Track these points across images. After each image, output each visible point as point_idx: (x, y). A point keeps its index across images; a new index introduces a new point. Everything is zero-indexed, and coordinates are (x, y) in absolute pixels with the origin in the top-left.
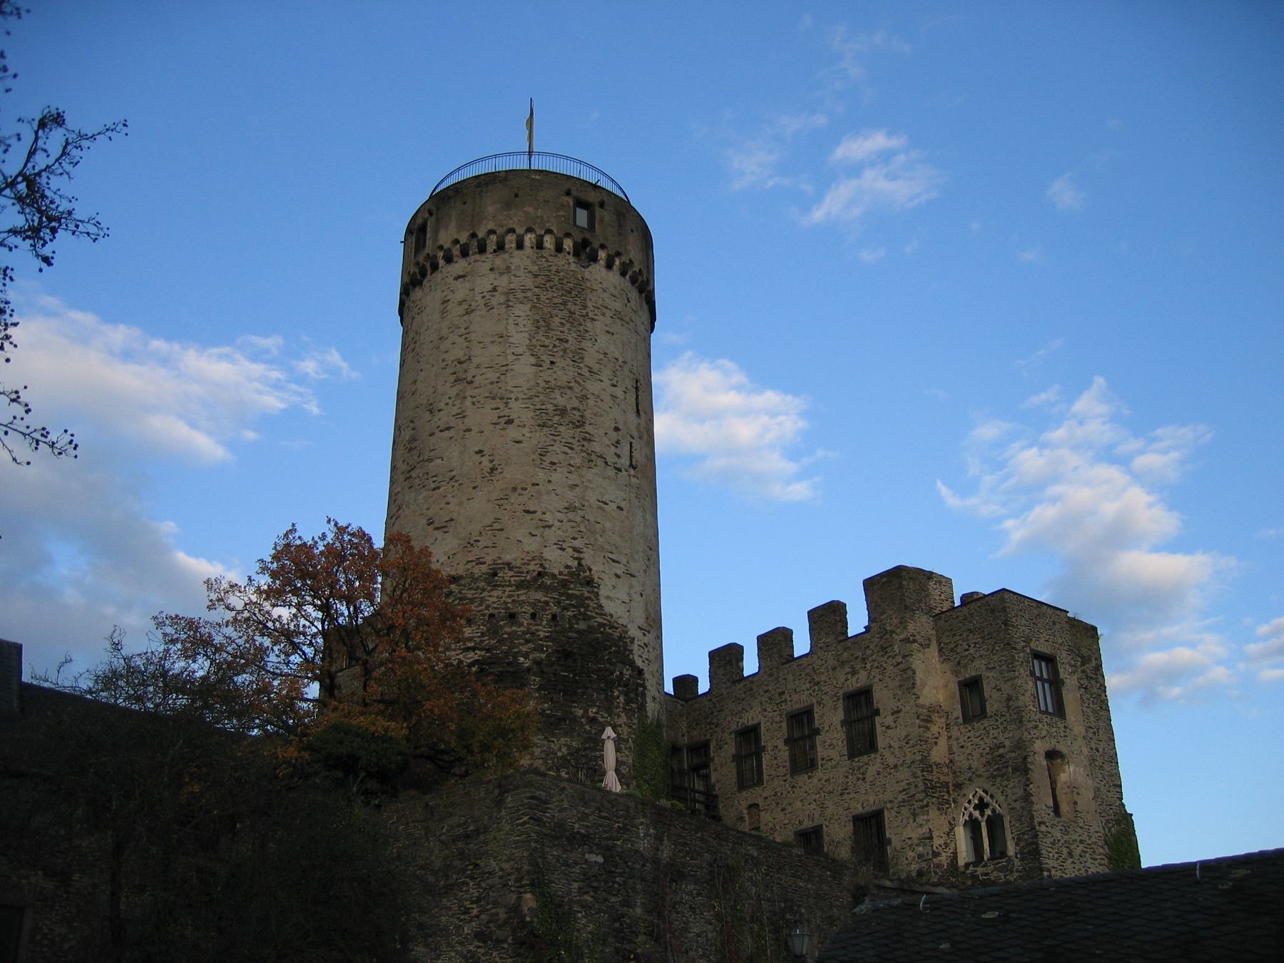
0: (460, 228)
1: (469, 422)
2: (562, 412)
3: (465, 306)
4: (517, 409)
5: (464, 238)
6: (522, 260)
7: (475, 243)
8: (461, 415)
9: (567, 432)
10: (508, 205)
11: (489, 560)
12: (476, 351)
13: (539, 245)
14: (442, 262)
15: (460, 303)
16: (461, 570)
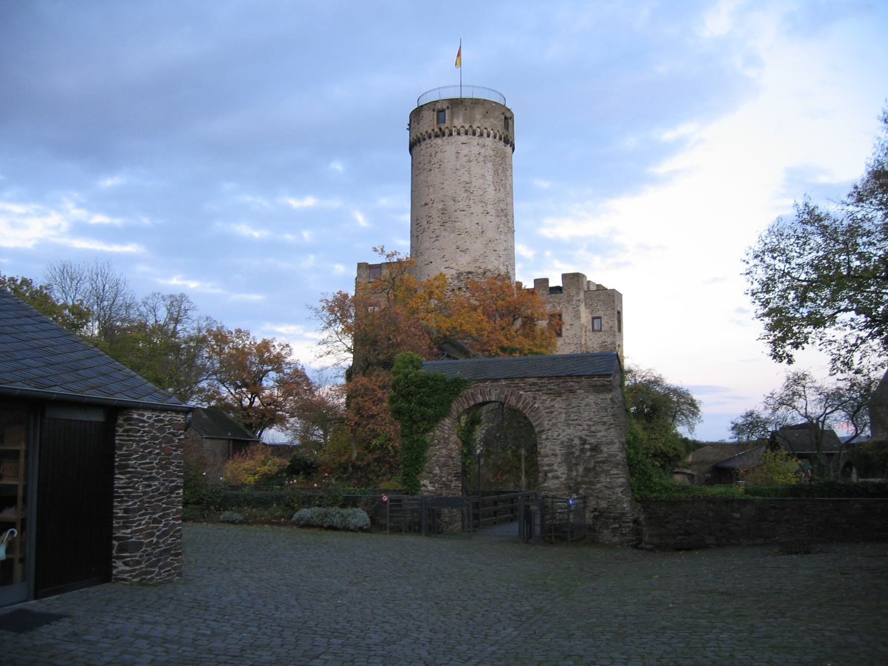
0: (465, 121)
1: (473, 210)
2: (502, 210)
3: (467, 158)
4: (490, 208)
5: (467, 127)
6: (489, 141)
7: (470, 131)
8: (469, 206)
9: (504, 219)
10: (484, 117)
11: (483, 267)
12: (474, 180)
13: (495, 137)
14: (454, 134)
15: (466, 156)
16: (473, 270)
